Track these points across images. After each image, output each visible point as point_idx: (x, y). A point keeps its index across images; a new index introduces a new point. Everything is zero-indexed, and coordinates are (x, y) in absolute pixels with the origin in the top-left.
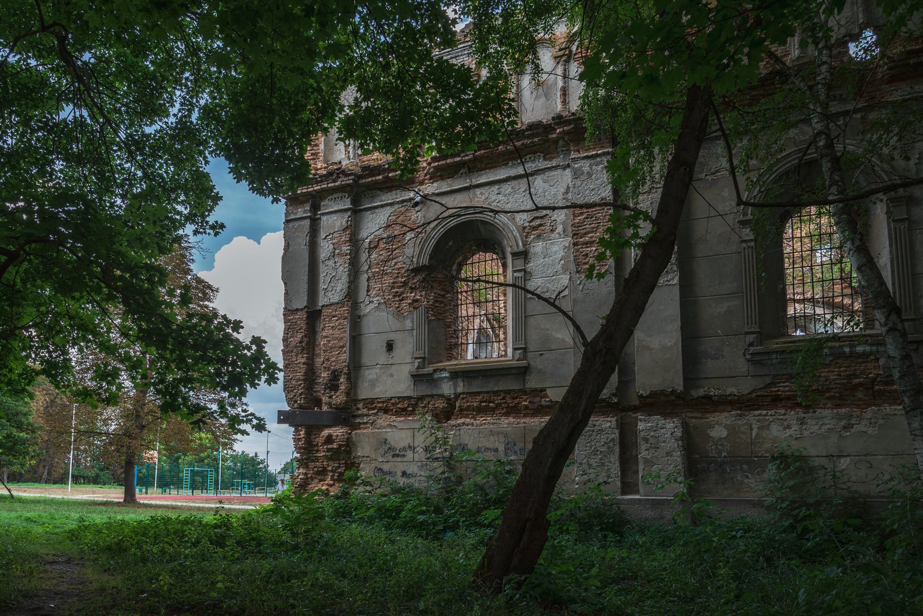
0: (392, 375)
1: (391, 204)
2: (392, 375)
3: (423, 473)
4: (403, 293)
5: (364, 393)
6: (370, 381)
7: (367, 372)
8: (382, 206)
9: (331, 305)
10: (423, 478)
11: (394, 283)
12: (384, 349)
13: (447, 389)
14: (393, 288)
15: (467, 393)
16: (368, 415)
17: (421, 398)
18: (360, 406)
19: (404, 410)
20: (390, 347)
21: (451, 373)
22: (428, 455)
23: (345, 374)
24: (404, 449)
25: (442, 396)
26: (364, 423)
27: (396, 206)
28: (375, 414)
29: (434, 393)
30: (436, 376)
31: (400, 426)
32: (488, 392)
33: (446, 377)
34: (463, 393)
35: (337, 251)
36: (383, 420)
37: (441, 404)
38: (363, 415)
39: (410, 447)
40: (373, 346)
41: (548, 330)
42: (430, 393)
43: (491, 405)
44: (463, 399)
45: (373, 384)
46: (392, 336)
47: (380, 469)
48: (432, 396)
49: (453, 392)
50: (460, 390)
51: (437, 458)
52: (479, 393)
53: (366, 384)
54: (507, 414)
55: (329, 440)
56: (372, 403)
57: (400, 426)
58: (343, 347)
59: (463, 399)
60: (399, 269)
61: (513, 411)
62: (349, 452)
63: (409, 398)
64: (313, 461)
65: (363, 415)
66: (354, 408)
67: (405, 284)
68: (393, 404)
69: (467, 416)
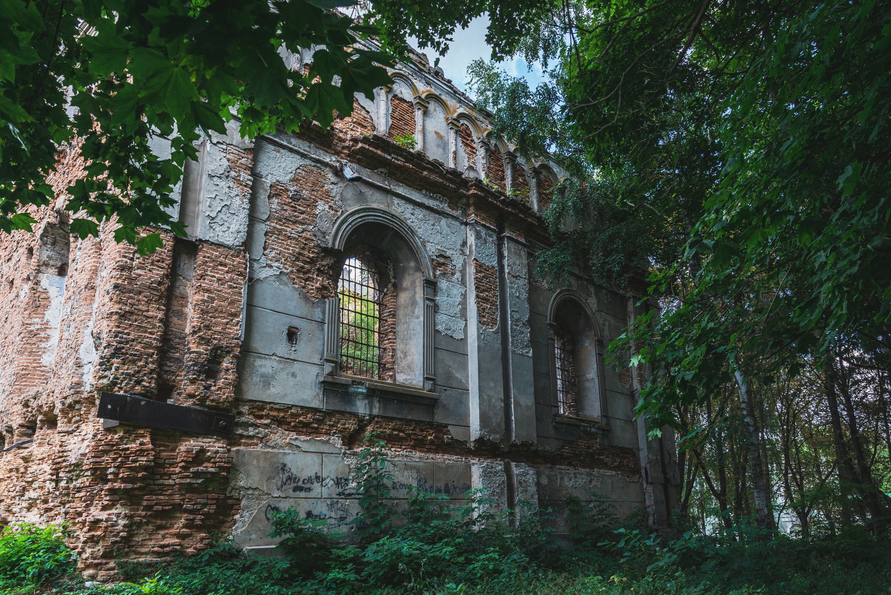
0: (294, 375)
1: (303, 156)
2: (294, 375)
3: (333, 515)
4: (308, 271)
5: (254, 392)
6: (262, 376)
7: (258, 362)
8: (291, 150)
9: (220, 245)
10: (333, 521)
11: (300, 254)
12: (284, 336)
13: (361, 408)
14: (297, 259)
15: (382, 417)
16: (256, 426)
17: (329, 414)
18: (245, 409)
19: (306, 425)
20: (292, 335)
21: (368, 389)
22: (340, 490)
23: (235, 357)
24: (310, 480)
25: (355, 415)
26: (249, 437)
27: (308, 162)
28: (267, 426)
29: (348, 410)
30: (351, 389)
31: (305, 447)
32: (400, 420)
33: (362, 393)
34: (378, 416)
35: (233, 174)
36: (279, 437)
37: (351, 425)
38: (246, 425)
39: (317, 478)
40: (271, 327)
41: (450, 367)
42: (342, 409)
43: (401, 434)
44: (377, 422)
45: (267, 381)
46: (296, 322)
48: (342, 413)
49: (368, 413)
50: (376, 411)
51: (350, 494)
52: (392, 419)
53: (256, 379)
54: (414, 447)
55: (200, 457)
56: (262, 409)
57: (305, 447)
58: (235, 315)
59: (377, 422)
60: (307, 239)
61: (419, 445)
62: (226, 480)
63: (315, 410)
64: (152, 493)
65: (246, 425)
66: (235, 411)
67: (312, 261)
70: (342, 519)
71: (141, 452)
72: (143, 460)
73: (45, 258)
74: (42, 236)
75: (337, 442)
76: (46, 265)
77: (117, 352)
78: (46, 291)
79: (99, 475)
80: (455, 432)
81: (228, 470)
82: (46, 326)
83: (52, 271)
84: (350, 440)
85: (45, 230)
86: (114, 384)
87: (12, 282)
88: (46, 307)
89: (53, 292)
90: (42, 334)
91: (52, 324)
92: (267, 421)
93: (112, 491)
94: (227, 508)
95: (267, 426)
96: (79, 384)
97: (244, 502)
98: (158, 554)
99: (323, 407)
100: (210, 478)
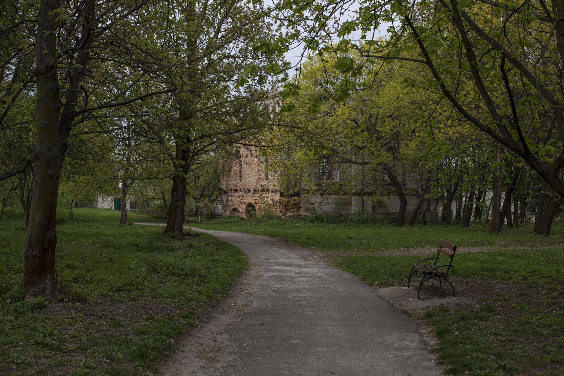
75: (319, 195)
79: (280, 203)
84: (322, 195)
94: (299, 208)
100: (296, 204)
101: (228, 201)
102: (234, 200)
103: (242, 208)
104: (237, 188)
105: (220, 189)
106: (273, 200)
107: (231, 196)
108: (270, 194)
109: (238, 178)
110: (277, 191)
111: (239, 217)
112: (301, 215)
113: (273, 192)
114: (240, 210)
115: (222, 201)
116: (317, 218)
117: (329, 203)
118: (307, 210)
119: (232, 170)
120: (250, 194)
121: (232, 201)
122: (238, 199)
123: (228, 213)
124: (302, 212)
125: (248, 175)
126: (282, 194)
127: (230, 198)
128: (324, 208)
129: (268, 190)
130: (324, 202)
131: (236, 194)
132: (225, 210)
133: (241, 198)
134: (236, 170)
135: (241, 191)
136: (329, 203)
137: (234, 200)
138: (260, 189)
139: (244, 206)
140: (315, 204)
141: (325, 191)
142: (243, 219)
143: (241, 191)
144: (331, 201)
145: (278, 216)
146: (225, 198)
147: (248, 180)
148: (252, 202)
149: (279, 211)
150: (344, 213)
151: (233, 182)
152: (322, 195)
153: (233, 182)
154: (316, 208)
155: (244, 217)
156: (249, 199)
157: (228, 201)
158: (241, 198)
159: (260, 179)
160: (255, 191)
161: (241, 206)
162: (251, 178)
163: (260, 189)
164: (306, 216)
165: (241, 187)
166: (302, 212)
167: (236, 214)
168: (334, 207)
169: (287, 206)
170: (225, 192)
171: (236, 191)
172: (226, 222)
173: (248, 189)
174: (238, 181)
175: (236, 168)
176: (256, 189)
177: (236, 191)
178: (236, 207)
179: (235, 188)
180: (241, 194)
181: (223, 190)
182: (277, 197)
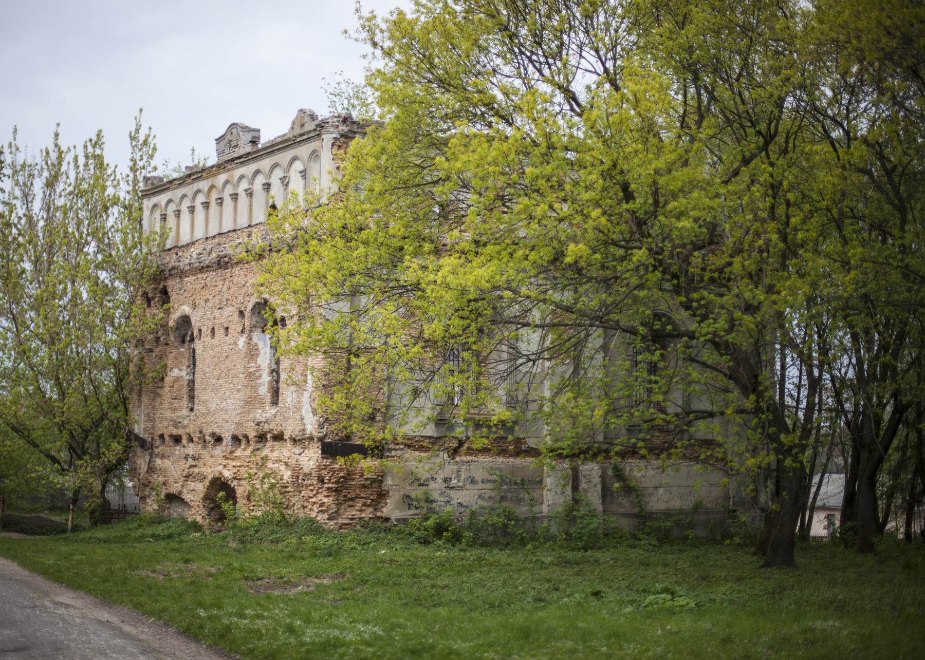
17: (438, 438)
24: (428, 480)
28: (402, 449)
36: (410, 454)
37: (454, 444)
47: (408, 497)
54: (498, 455)
62: (381, 481)
63: (430, 437)
64: (346, 488)
65: (390, 450)
68: (416, 441)
69: (471, 455)
70: (448, 502)
71: (341, 470)
72: (342, 474)
73: (254, 323)
74: (252, 309)
76: (255, 326)
77: (327, 420)
78: (256, 345)
79: (321, 480)
80: (532, 443)
81: (382, 476)
82: (258, 369)
83: (260, 330)
85: (255, 306)
86: (326, 435)
87: (227, 328)
88: (257, 355)
89: (261, 345)
90: (257, 374)
91: (262, 367)
92: (402, 447)
93: (328, 488)
94: (382, 495)
95: (402, 449)
96: (304, 430)
97: (391, 493)
98: (352, 519)
99: (435, 435)
101: (151, 469)
102: (172, 467)
103: (194, 493)
104: (180, 432)
105: (131, 436)
106: (297, 471)
107: (163, 457)
108: (286, 451)
109: (185, 402)
110: (311, 438)
111: (184, 520)
112: (387, 519)
113: (294, 441)
114: (187, 497)
115: (133, 472)
116: (439, 530)
117: (473, 481)
118: (408, 501)
119: (167, 379)
120: (218, 451)
121: (163, 471)
122: (184, 465)
123: (151, 506)
124: (391, 509)
125: (215, 389)
126: (330, 450)
127: (158, 461)
128: (458, 497)
129: (279, 437)
130: (458, 476)
131: (178, 450)
132: (143, 498)
133: (191, 462)
134: (177, 379)
135: (191, 440)
136: (473, 481)
137: (172, 467)
138: (252, 434)
139: (200, 488)
140: (432, 484)
141: (461, 443)
142: (196, 527)
143: (191, 440)
144: (479, 475)
145: (312, 521)
146: (142, 463)
147: (213, 407)
148: (227, 474)
149: (315, 505)
150: (523, 510)
151: (168, 414)
152: (455, 452)
153: (168, 414)
154: (435, 495)
155: (199, 519)
156: (216, 464)
157: (151, 469)
158: (191, 462)
159: (252, 402)
160: (236, 439)
161: (192, 485)
162: (224, 399)
163: (252, 434)
164: (405, 521)
165: (191, 429)
166: (391, 509)
167: (176, 511)
168: (488, 494)
169: (342, 489)
170: (143, 443)
171: (177, 439)
172: (143, 536)
173: (213, 434)
174: (185, 412)
175: (178, 373)
176: (239, 433)
177: (177, 439)
178: (174, 488)
179: (175, 432)
180: (191, 449)
181: (137, 438)
182: (311, 458)
